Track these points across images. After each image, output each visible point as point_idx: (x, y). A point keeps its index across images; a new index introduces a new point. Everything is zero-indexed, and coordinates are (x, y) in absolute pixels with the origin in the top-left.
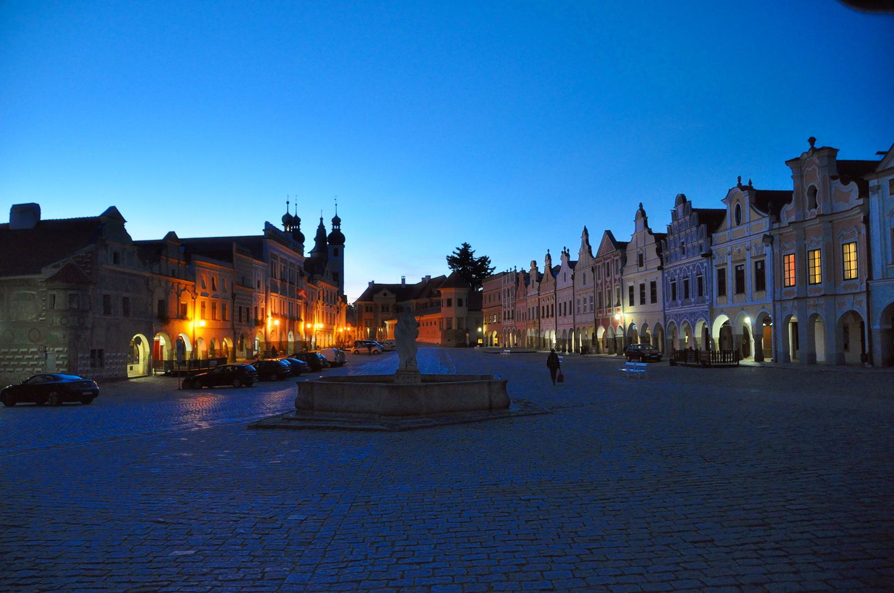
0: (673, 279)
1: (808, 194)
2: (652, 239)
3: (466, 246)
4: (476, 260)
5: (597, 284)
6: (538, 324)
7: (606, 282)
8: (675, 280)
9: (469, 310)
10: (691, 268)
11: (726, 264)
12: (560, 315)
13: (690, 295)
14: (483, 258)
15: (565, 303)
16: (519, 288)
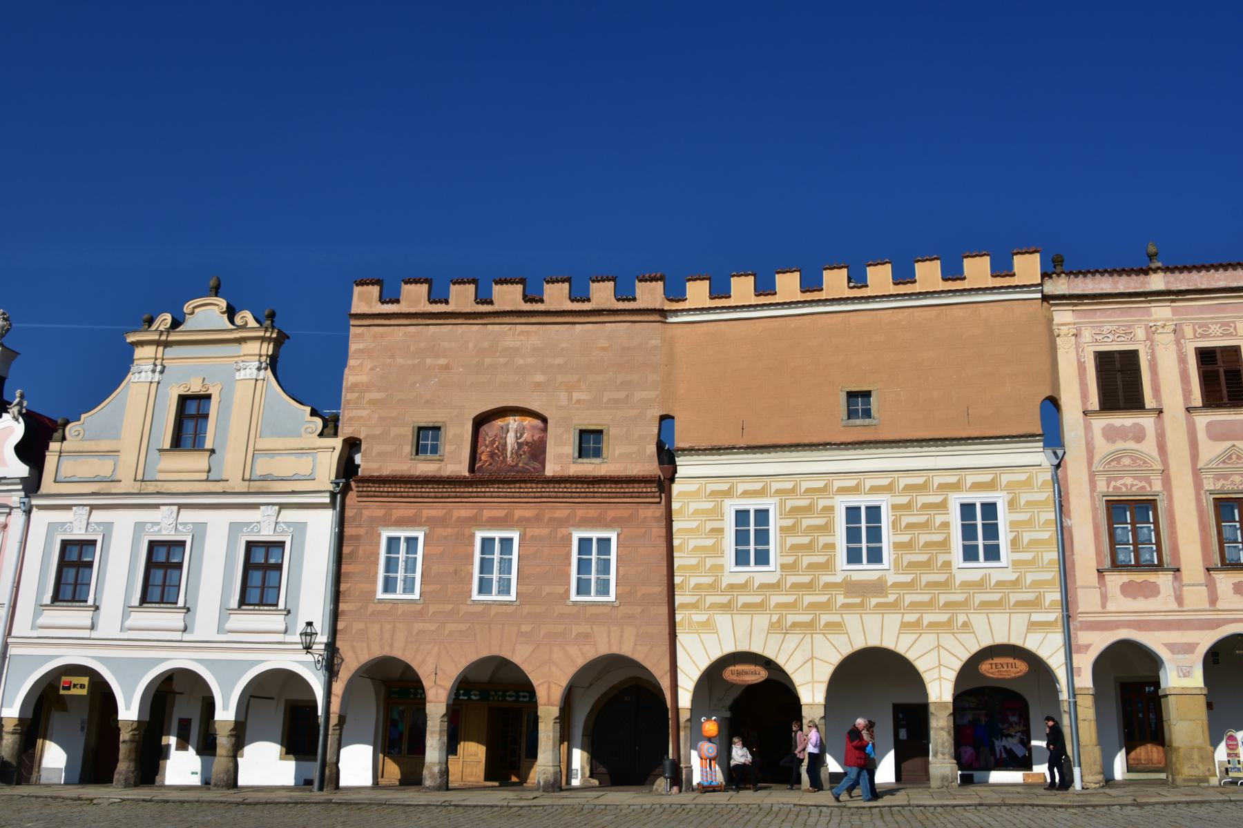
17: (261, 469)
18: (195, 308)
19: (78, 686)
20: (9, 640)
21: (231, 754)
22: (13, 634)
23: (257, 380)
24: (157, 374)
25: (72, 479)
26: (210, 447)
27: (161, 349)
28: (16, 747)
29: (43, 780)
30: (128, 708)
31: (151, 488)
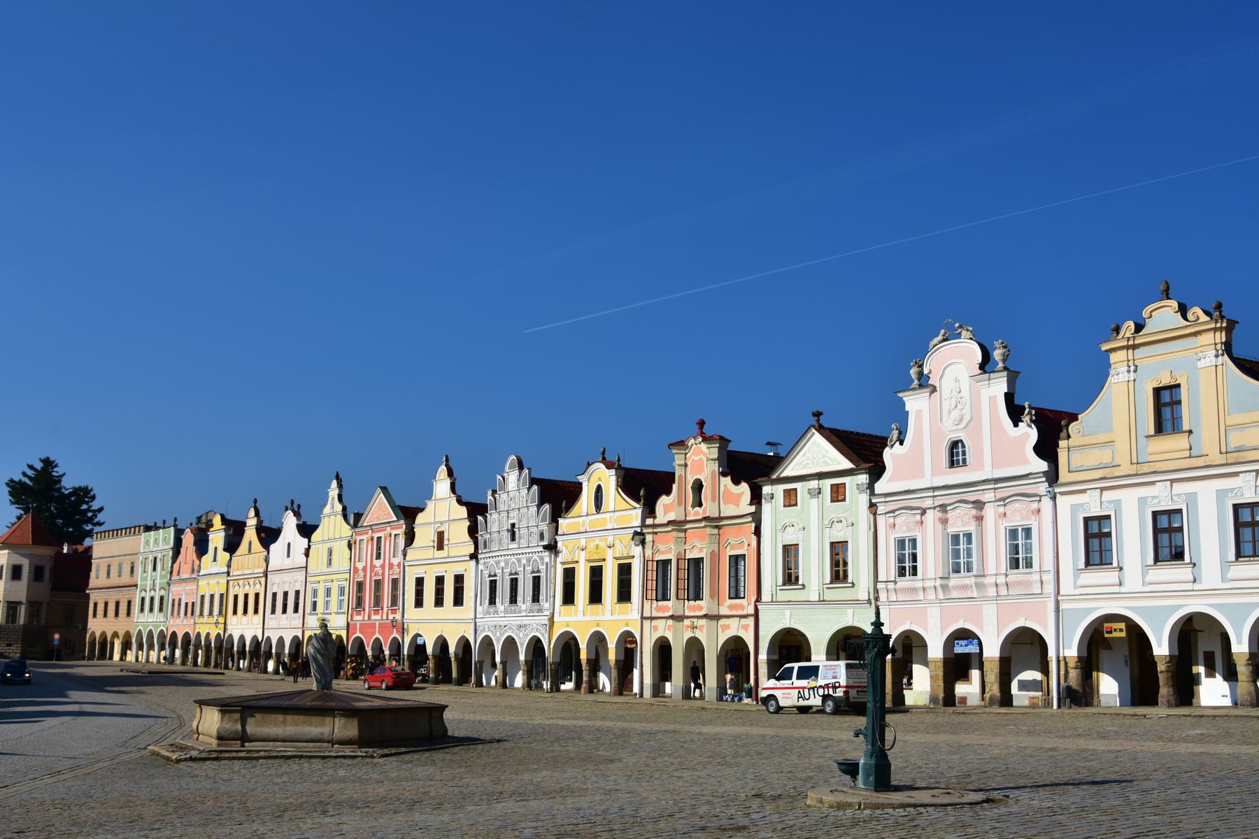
0: (493, 574)
1: (692, 488)
2: (463, 512)
3: (48, 463)
4: (67, 492)
5: (356, 570)
6: (223, 626)
7: (373, 567)
8: (495, 575)
9: (53, 589)
10: (524, 561)
11: (577, 562)
12: (273, 612)
13: (520, 598)
14: (80, 489)
15: (286, 594)
16: (181, 558)
17: (1233, 444)
18: (1151, 312)
19: (1118, 630)
20: (1059, 598)
21: (1251, 679)
22: (1061, 593)
23: (1216, 366)
24: (1132, 373)
25: (1080, 469)
26: (1188, 429)
27: (1130, 351)
28: (1080, 678)
29: (1103, 704)
30: (1160, 645)
31: (1146, 468)
